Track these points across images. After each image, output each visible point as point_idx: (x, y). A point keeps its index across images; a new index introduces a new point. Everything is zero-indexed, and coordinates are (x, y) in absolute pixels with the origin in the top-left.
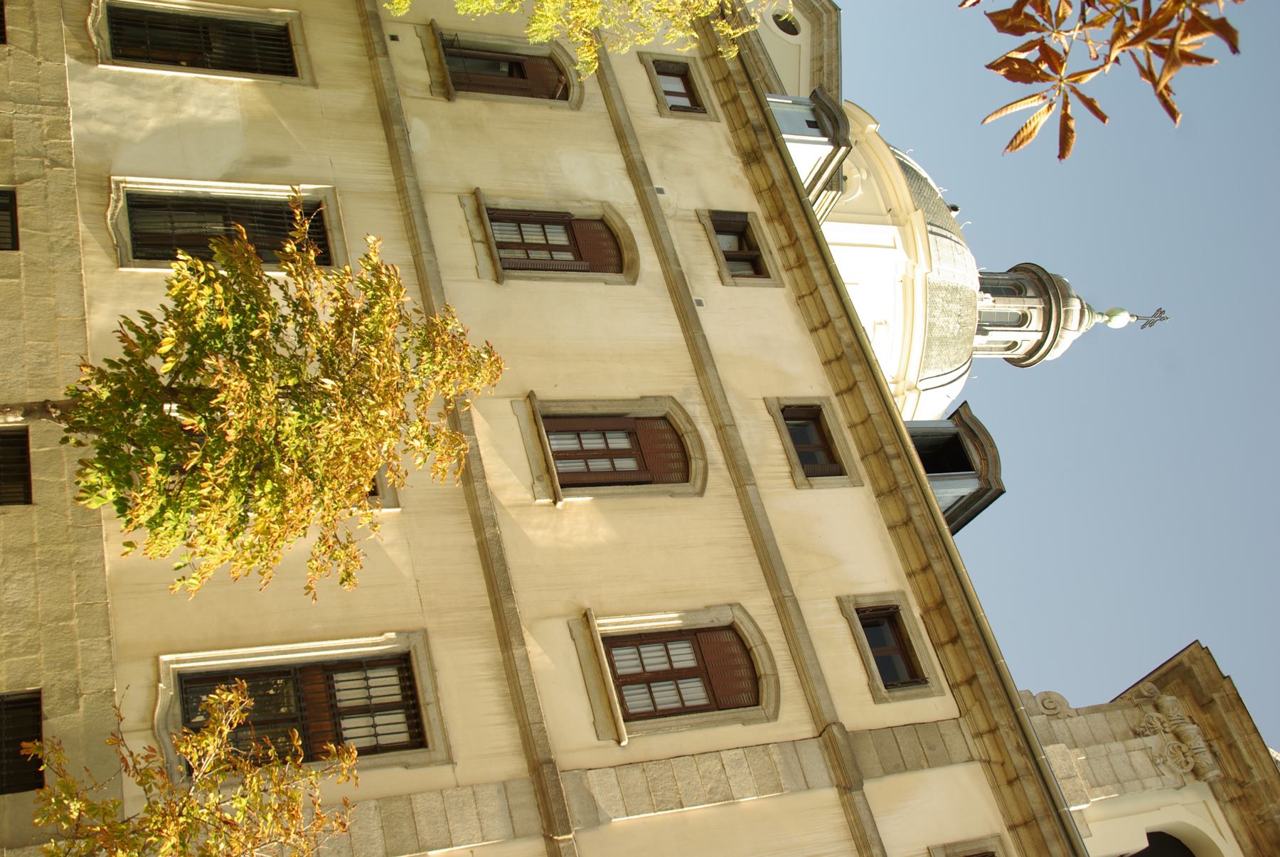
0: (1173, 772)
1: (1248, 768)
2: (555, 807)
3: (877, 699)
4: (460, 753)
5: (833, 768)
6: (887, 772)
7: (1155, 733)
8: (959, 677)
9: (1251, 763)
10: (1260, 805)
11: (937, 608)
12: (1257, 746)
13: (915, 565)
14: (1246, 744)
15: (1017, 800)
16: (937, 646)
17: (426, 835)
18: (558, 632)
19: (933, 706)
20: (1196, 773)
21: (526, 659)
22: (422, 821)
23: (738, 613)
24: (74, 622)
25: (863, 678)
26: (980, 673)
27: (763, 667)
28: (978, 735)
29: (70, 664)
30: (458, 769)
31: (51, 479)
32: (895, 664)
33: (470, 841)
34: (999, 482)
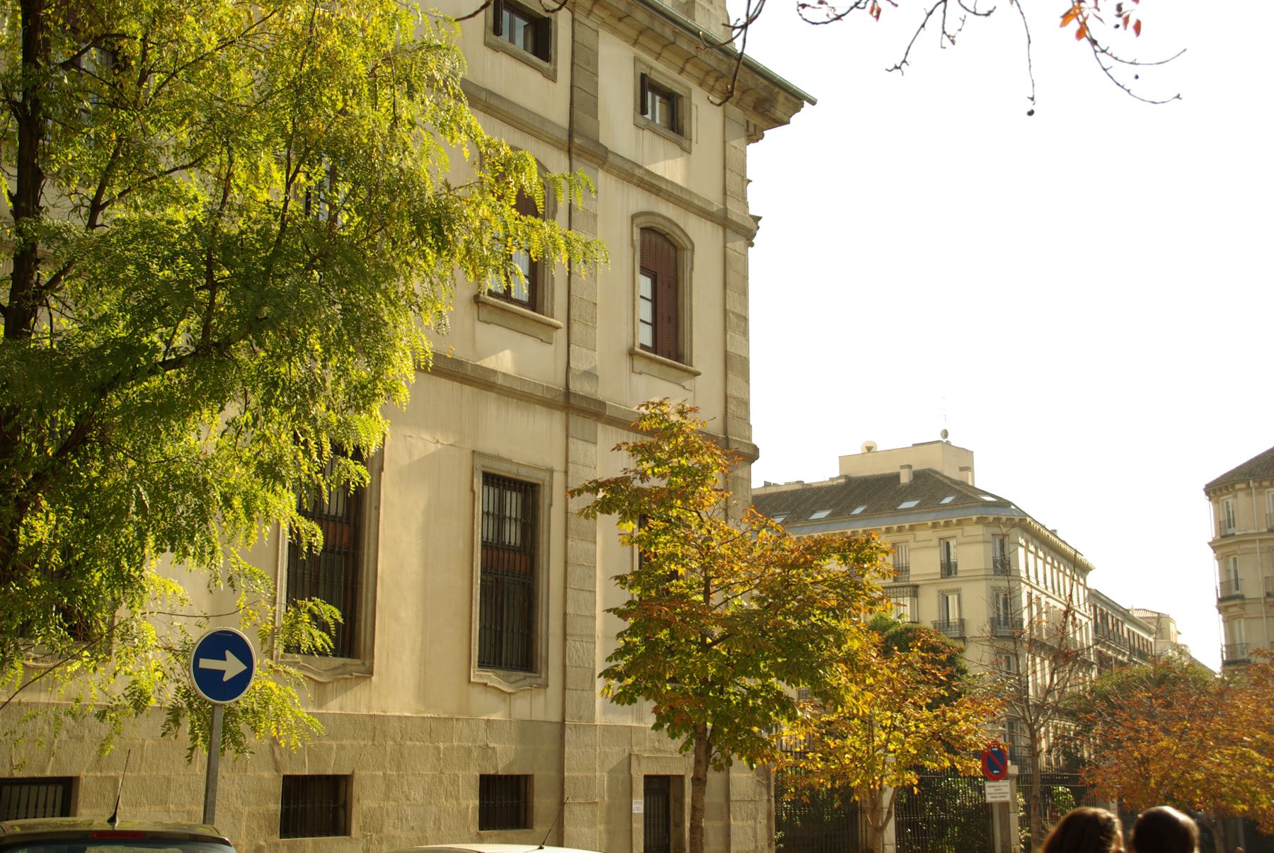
18: (489, 334)
21: (505, 375)
24: (441, 745)
28: (590, 12)
29: (469, 751)
31: (334, 756)
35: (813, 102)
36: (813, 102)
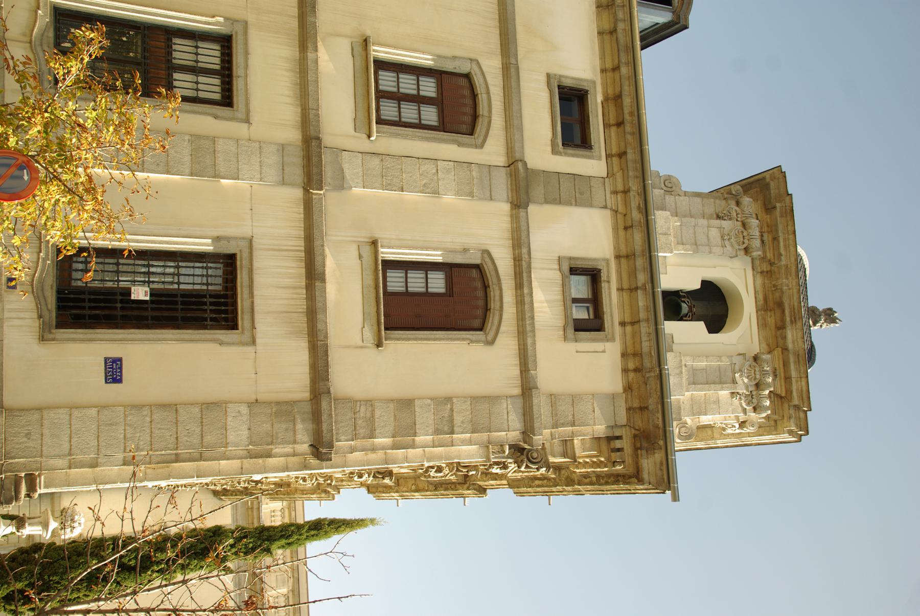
0: (732, 246)
1: (781, 255)
2: (315, 170)
3: (554, 152)
4: (255, 117)
5: (512, 190)
6: (547, 202)
7: (730, 219)
8: (614, 151)
9: (782, 251)
10: (778, 279)
11: (614, 99)
12: (791, 242)
13: (609, 65)
14: (785, 240)
15: (626, 240)
16: (607, 126)
17: (222, 167)
18: (343, 48)
19: (591, 166)
20: (747, 250)
21: (316, 62)
22: (220, 158)
23: (475, 67)
25: (549, 135)
26: (629, 151)
27: (482, 109)
28: (615, 192)
30: (251, 127)
32: (574, 130)
33: (251, 179)
34: (686, 19)
35: (675, 498)
36: (675, 498)
